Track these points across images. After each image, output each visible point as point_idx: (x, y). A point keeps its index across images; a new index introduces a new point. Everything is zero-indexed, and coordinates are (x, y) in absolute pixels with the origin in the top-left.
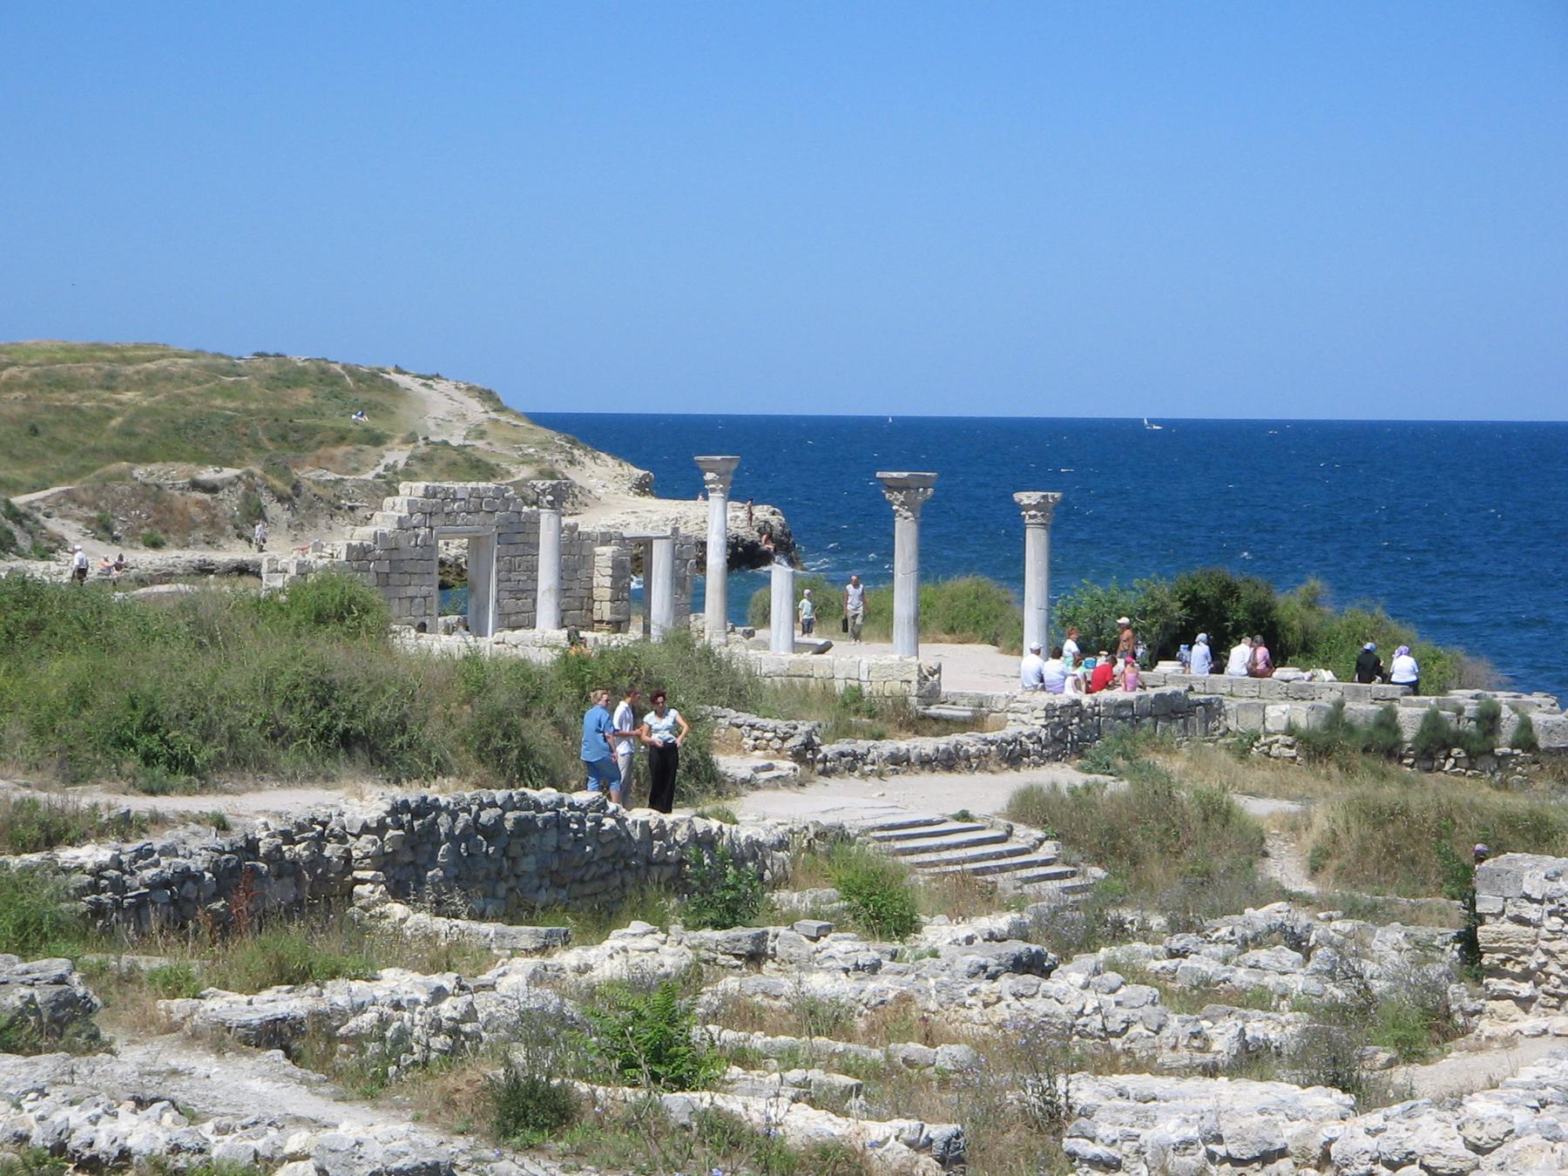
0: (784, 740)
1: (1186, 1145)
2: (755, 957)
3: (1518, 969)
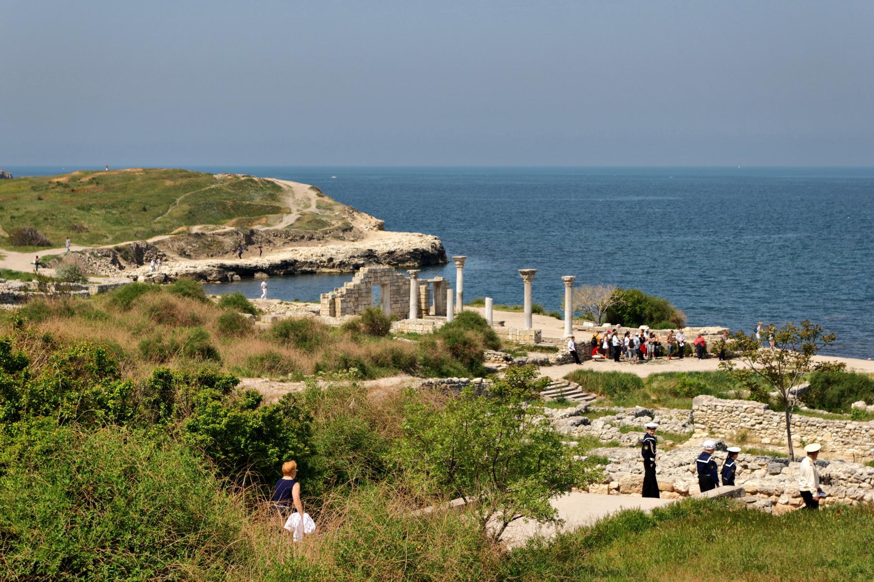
1: (633, 459)
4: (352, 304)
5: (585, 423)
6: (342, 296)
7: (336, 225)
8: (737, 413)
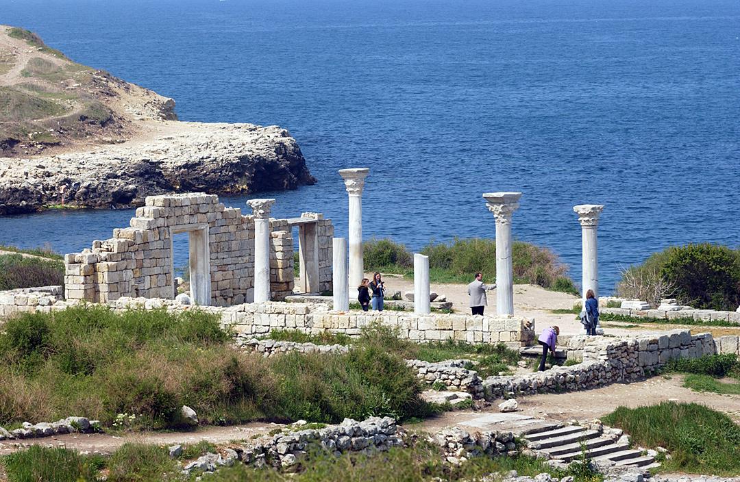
0: (461, 379)
4: (130, 273)
6: (110, 258)
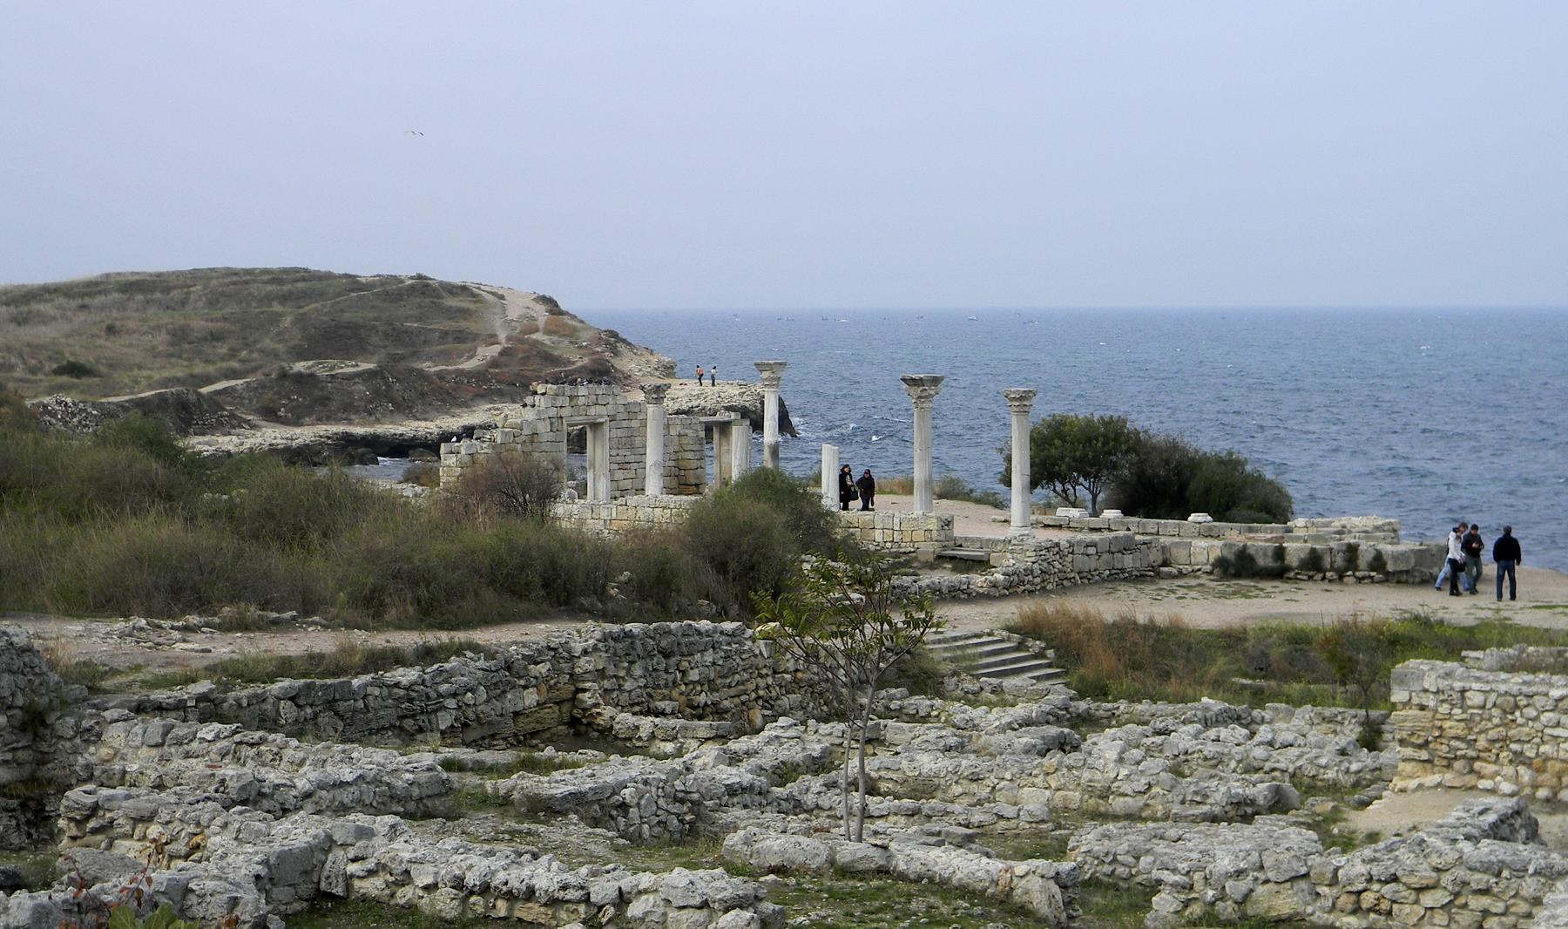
1: (1239, 873)
2: (875, 741)
3: (1420, 741)
5: (1064, 745)
7: (579, 364)
8: (1531, 712)
